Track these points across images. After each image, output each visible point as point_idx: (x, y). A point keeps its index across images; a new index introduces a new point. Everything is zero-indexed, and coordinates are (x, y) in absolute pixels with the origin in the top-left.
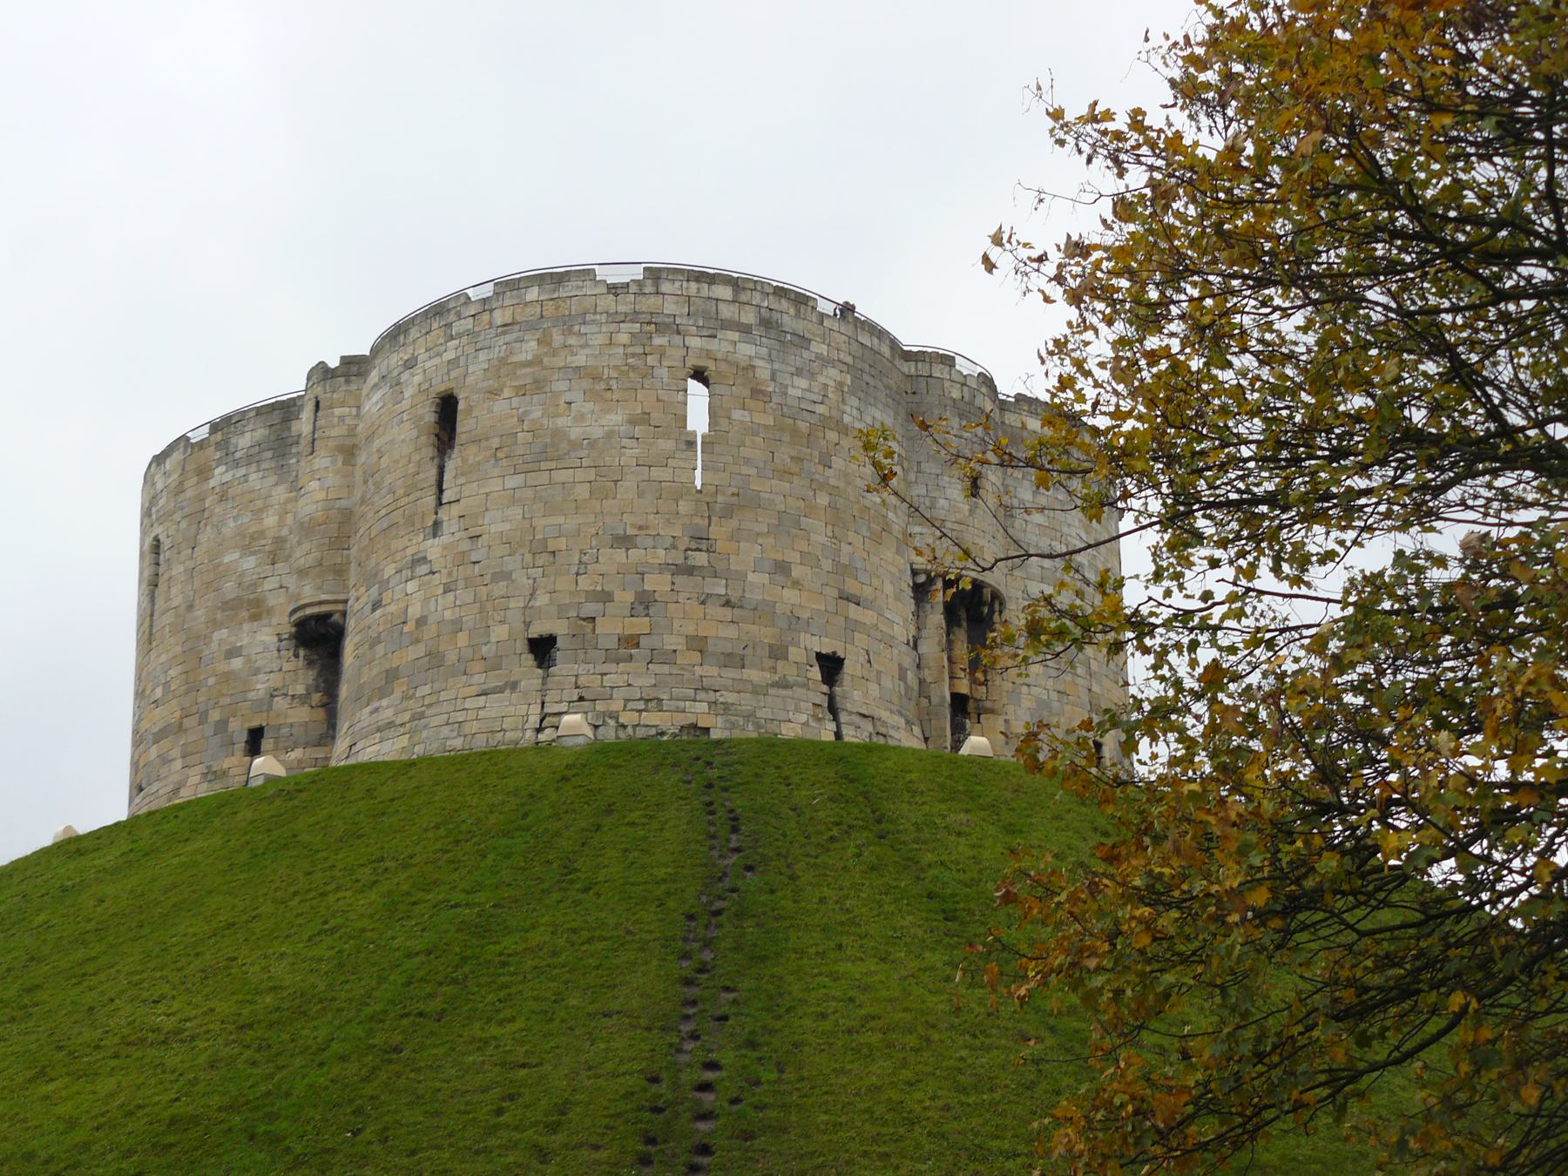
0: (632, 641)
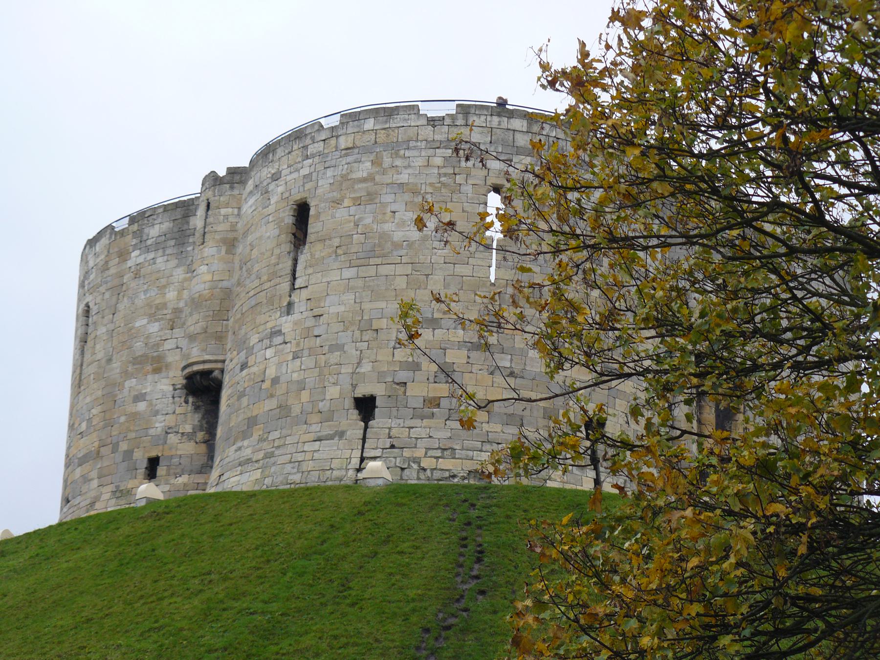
0: (435, 402)
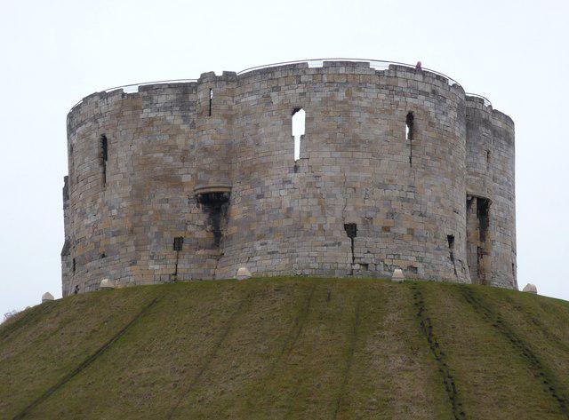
0: (386, 229)
